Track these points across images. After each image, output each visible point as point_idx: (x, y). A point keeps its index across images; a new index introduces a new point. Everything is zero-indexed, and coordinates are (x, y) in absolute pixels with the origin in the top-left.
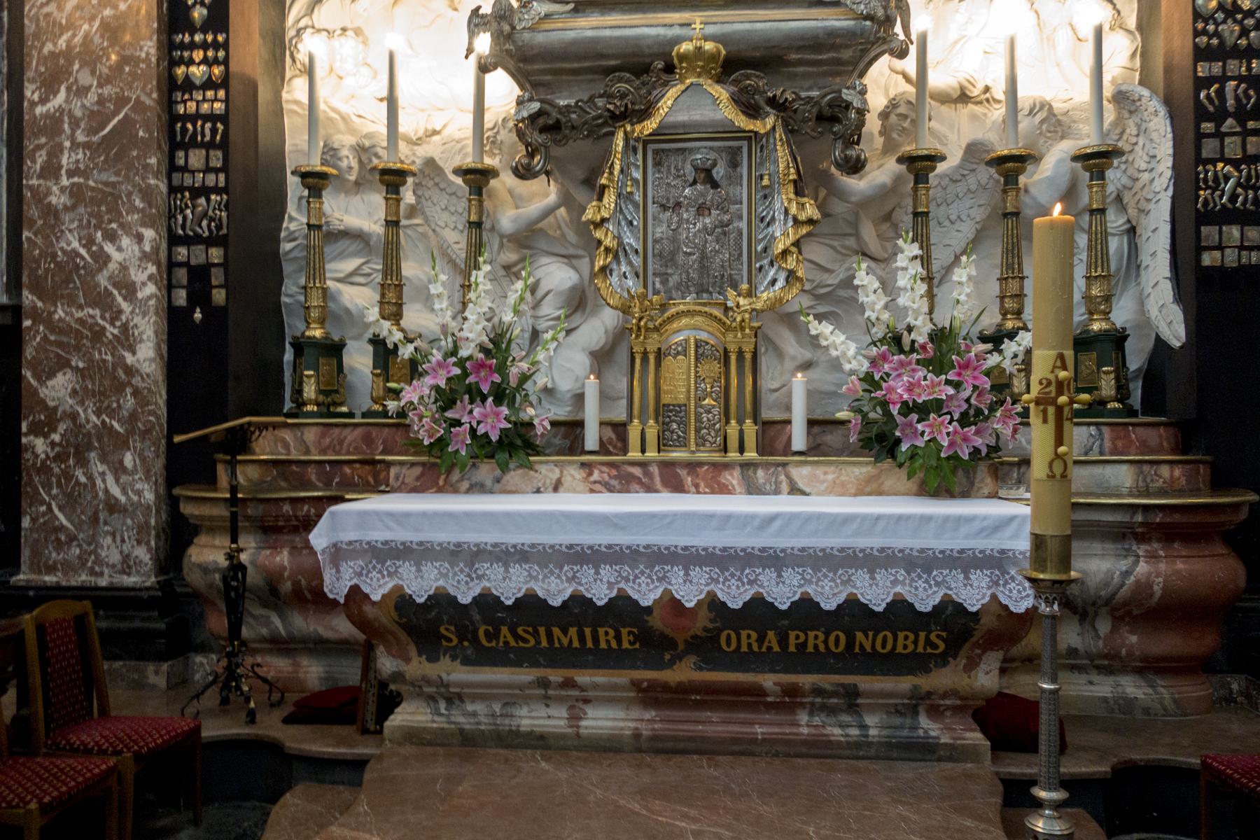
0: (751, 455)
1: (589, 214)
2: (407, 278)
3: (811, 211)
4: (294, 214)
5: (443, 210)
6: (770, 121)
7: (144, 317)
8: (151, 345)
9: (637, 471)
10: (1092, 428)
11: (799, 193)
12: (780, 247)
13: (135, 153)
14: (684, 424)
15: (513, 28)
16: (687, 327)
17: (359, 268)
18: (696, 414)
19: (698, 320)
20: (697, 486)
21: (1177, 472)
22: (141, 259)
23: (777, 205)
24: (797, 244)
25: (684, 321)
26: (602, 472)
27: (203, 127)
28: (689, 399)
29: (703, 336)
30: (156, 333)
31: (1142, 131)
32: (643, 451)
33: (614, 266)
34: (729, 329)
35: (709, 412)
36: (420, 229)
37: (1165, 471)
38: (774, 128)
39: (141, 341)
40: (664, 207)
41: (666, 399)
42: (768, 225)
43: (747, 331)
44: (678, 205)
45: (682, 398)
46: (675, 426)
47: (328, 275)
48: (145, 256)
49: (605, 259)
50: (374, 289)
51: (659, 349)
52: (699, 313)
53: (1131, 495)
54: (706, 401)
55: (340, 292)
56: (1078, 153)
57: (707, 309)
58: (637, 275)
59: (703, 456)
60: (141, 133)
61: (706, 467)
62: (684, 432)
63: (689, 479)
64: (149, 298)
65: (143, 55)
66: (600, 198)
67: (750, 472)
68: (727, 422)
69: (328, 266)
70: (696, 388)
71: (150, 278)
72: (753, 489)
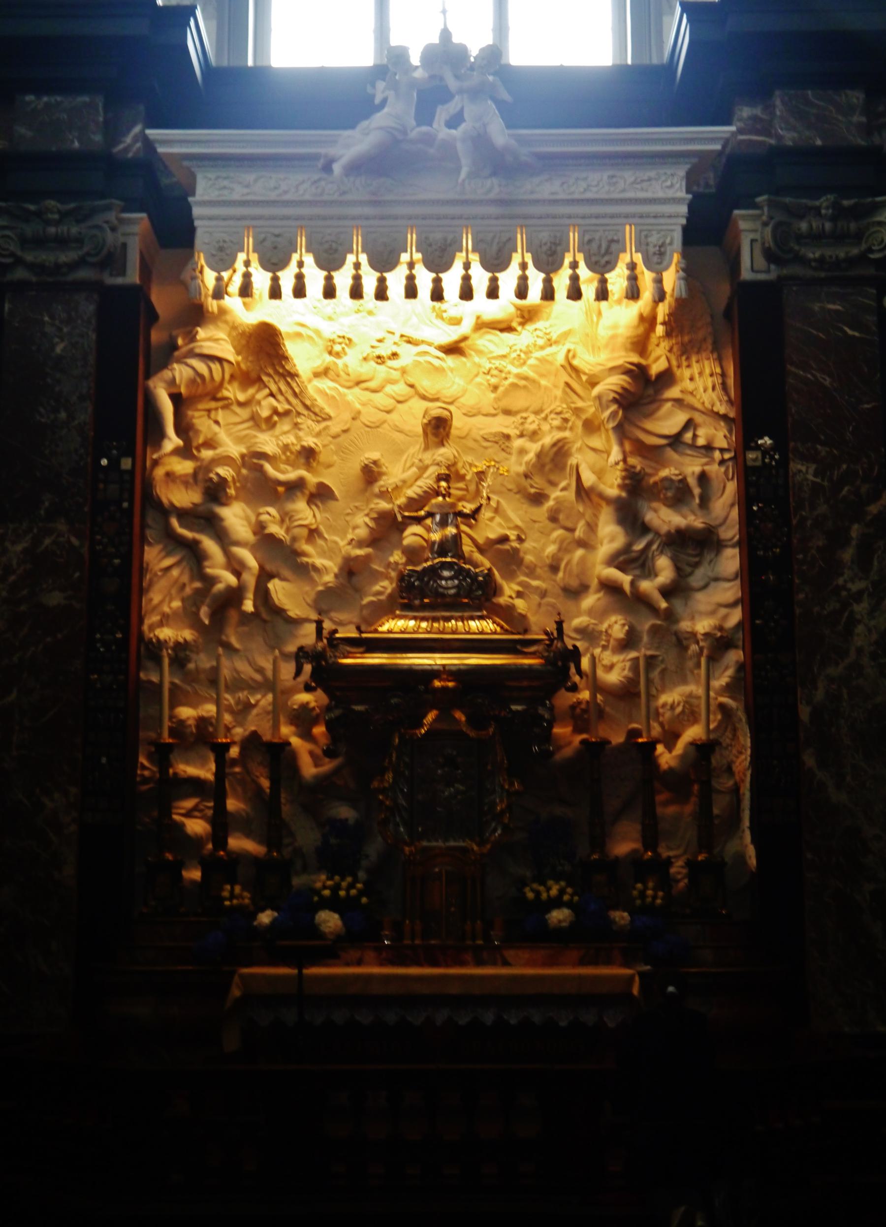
1: (375, 784)
4: (146, 763)
6: (491, 730)
15: (326, 661)
17: (196, 806)
47: (174, 811)
54: (453, 909)
72: (480, 963)
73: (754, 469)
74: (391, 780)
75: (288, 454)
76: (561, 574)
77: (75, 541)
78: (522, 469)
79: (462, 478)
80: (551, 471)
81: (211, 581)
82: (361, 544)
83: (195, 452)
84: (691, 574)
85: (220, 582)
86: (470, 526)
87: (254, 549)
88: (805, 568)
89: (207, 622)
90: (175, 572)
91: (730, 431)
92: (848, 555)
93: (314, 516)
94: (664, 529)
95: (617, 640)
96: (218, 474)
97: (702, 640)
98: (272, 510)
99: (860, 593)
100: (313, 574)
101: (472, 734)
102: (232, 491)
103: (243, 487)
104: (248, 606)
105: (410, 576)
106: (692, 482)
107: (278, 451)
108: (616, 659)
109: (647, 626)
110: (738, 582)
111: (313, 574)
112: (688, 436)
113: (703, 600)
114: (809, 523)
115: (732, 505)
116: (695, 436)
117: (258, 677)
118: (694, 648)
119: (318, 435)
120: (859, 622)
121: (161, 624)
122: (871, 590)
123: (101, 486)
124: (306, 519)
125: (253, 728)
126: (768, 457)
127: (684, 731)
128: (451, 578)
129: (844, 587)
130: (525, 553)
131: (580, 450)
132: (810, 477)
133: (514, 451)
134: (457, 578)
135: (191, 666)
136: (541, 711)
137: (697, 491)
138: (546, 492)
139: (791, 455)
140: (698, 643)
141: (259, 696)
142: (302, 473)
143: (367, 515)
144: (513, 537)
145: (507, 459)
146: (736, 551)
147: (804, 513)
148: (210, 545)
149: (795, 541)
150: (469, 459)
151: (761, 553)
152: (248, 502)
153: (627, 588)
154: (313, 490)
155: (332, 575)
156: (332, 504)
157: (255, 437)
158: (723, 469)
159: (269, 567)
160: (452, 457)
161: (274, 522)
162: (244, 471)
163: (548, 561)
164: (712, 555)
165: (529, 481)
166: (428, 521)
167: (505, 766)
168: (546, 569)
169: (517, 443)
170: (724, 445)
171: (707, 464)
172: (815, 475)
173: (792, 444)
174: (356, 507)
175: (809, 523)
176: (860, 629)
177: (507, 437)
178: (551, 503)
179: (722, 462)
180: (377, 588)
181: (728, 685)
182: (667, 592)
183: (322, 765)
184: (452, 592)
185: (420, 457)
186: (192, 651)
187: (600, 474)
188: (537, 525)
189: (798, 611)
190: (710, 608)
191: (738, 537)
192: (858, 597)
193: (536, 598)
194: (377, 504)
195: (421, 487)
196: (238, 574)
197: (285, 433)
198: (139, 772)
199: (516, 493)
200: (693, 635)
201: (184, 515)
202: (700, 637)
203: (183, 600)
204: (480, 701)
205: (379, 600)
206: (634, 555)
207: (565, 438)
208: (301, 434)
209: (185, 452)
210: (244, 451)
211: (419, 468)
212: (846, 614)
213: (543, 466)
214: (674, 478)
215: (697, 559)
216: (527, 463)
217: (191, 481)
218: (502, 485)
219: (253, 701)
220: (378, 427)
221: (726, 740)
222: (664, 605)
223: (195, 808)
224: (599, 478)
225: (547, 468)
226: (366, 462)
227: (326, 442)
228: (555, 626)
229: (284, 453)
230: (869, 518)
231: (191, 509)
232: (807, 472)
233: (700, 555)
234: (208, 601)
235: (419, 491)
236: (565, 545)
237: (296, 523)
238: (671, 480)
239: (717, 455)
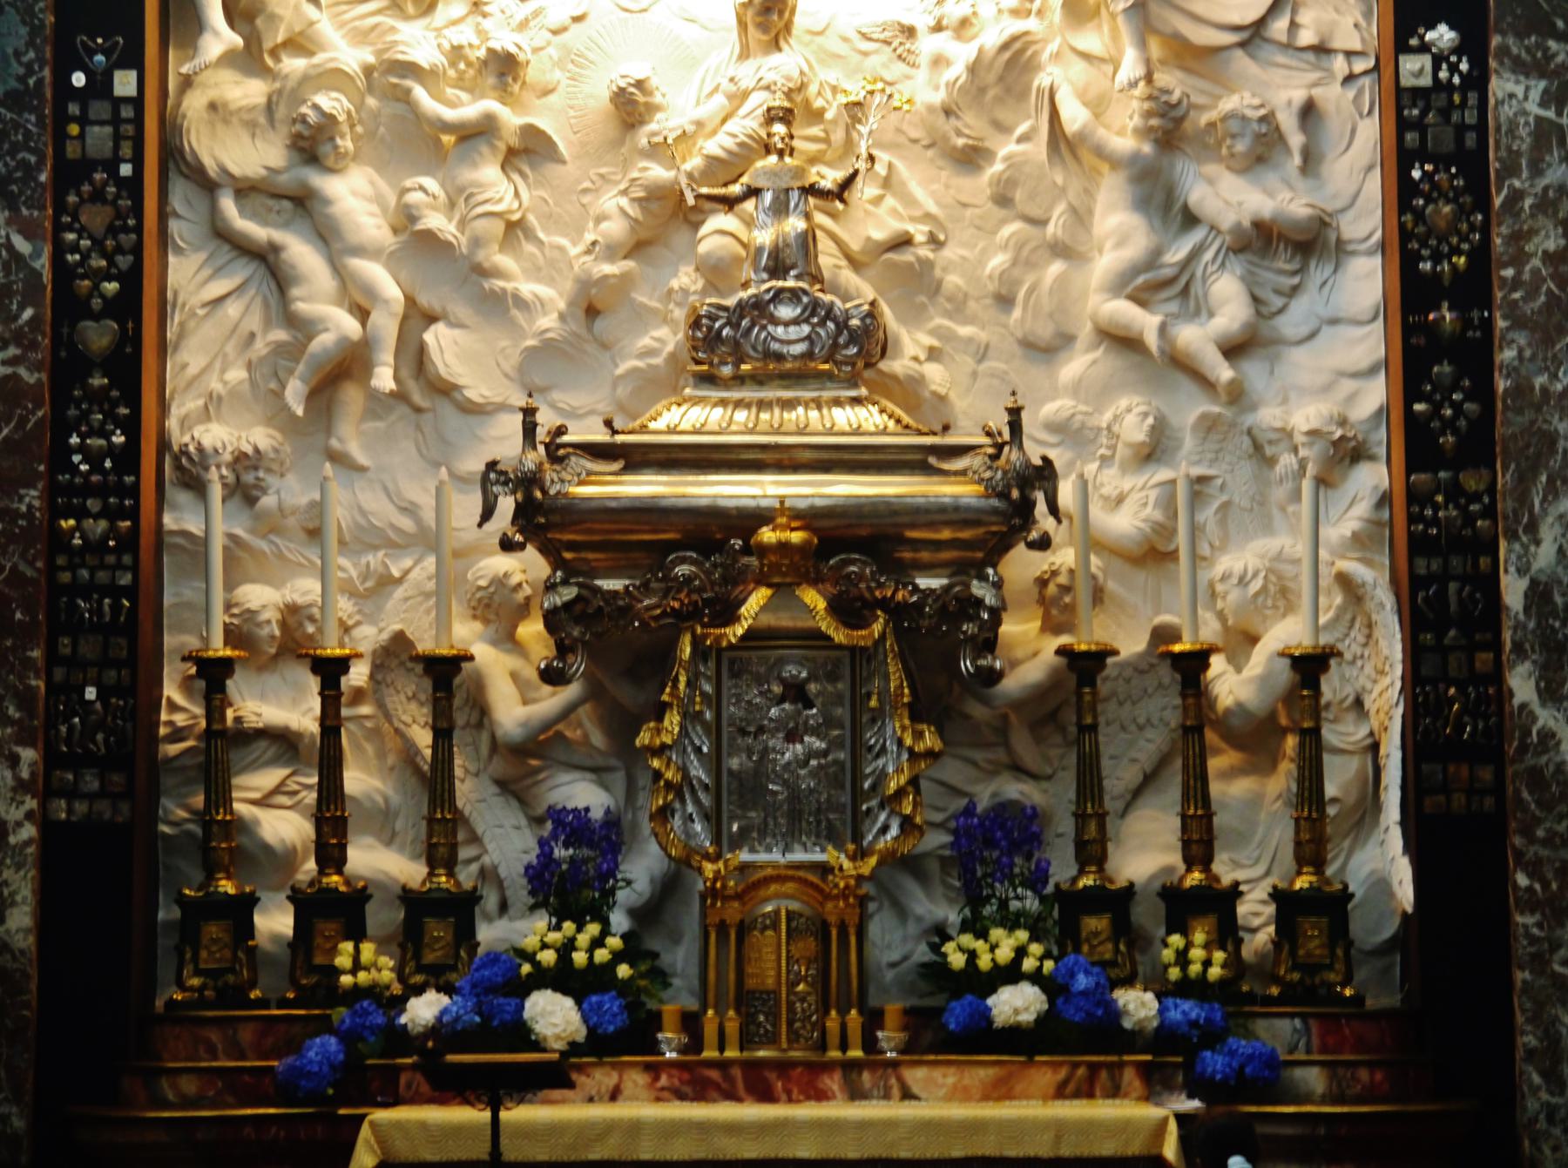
0: (856, 1053)
2: (353, 799)
3: (930, 740)
4: (179, 699)
5: (409, 699)
6: (877, 628)
7: (18, 870)
8: (27, 909)
9: (714, 1074)
11: (915, 717)
12: (893, 786)
13: (9, 643)
14: (774, 1016)
15: (544, 492)
16: (777, 896)
17: (282, 783)
18: (788, 1002)
19: (790, 887)
20: (789, 1093)
22: (14, 790)
23: (889, 732)
24: (914, 782)
25: (773, 888)
26: (670, 1076)
27: (100, 603)
28: (779, 983)
29: (795, 906)
30: (33, 891)
32: (722, 1049)
33: (677, 805)
34: (828, 897)
35: (803, 1000)
36: (369, 724)
37: (1364, 1074)
38: (883, 636)
39: (13, 904)
40: (743, 732)
41: (751, 983)
42: (878, 756)
43: (851, 900)
44: (761, 730)
45: (770, 982)
46: (762, 1018)
47: (234, 795)
48: (21, 787)
49: (665, 798)
50: (302, 814)
51: (742, 921)
52: (792, 879)
53: (1324, 1100)
54: (801, 987)
55: (257, 822)
57: (801, 874)
58: (706, 817)
59: (795, 1054)
60: (18, 616)
61: (799, 1070)
62: (774, 1025)
63: (780, 1084)
64: (27, 843)
65: (24, 508)
66: (660, 719)
67: (854, 1076)
68: (827, 1012)
69: (236, 781)
70: (788, 972)
71: (29, 815)
72: (856, 1094)
73: (1417, 93)
74: (677, 730)
75: (462, 66)
76: (1017, 313)
77: (22, 245)
78: (938, 97)
79: (817, 116)
80: (999, 100)
81: (303, 328)
82: (612, 252)
83: (269, 61)
84: (1281, 311)
85: (326, 330)
86: (833, 215)
87: (392, 261)
88: (1517, 295)
89: (300, 412)
90: (233, 309)
91: (1367, 15)
93: (517, 194)
94: (1227, 220)
95: (1129, 445)
96: (316, 107)
97: (1303, 444)
98: (430, 183)
100: (515, 312)
101: (840, 636)
102: (346, 143)
103: (371, 134)
104: (384, 379)
105: (713, 318)
106: (1288, 122)
107: (440, 60)
108: (1127, 483)
109: (1192, 417)
111: (515, 312)
112: (1279, 27)
113: (1303, 364)
114: (1528, 202)
115: (1370, 168)
116: (1294, 26)
117: (406, 524)
118: (1287, 461)
119: (523, 25)
121: (206, 415)
123: (74, 129)
124: (500, 200)
125: (397, 627)
126: (1444, 66)
128: (796, 322)
130: (945, 270)
131: (1056, 56)
132: (1533, 108)
133: (924, 60)
134: (807, 321)
135: (268, 501)
136: (978, 589)
137: (1296, 140)
138: (987, 144)
139: (1493, 64)
140: (1295, 450)
141: (408, 563)
142: (491, 105)
143: (624, 192)
144: (920, 238)
145: (908, 77)
146: (1377, 261)
147: (1517, 184)
148: (301, 252)
149: (1498, 241)
150: (831, 75)
151: (1426, 266)
152: (380, 168)
153: (1152, 340)
154: (514, 141)
155: (555, 315)
156: (553, 170)
157: (393, 29)
158: (1351, 93)
159: (424, 300)
160: (796, 74)
161: (435, 208)
162: (371, 102)
163: (992, 287)
164: (1329, 269)
165: (953, 121)
166: (749, 205)
167: (906, 700)
168: (988, 301)
169: (928, 44)
170: (1357, 46)
171: (1315, 85)
172: (1543, 104)
173: (1496, 40)
174: (602, 176)
175: (1528, 202)
177: (910, 32)
178: (998, 167)
179: (1350, 78)
180: (646, 341)
181: (1356, 536)
182: (1233, 350)
183: (535, 701)
184: (798, 349)
185: (730, 74)
186: (269, 470)
187: (1097, 105)
188: (969, 212)
189: (1501, 384)
193: (968, 362)
194: (645, 169)
195: (735, 136)
196: (363, 314)
197: (455, 23)
198: (164, 717)
199: (928, 147)
200: (1287, 434)
201: (246, 190)
202: (1299, 439)
203: (249, 366)
204: (853, 568)
205: (650, 366)
206: (1167, 272)
207: (1026, 33)
208: (487, 24)
209: (250, 59)
210: (371, 59)
211: (730, 97)
213: (982, 90)
214: (1250, 113)
215: (1296, 280)
216: (950, 86)
217: (262, 120)
218: (899, 131)
219: (396, 573)
220: (645, 10)
221: (1350, 648)
222: (1224, 372)
223: (277, 790)
224: (1097, 116)
225: (991, 93)
226: (623, 84)
227: (538, 43)
228: (1006, 418)
229: (453, 64)
231: (263, 179)
232: (1526, 98)
233: (1302, 270)
234: (301, 368)
235: (730, 143)
236: (1025, 253)
237: (480, 210)
238: (1244, 118)
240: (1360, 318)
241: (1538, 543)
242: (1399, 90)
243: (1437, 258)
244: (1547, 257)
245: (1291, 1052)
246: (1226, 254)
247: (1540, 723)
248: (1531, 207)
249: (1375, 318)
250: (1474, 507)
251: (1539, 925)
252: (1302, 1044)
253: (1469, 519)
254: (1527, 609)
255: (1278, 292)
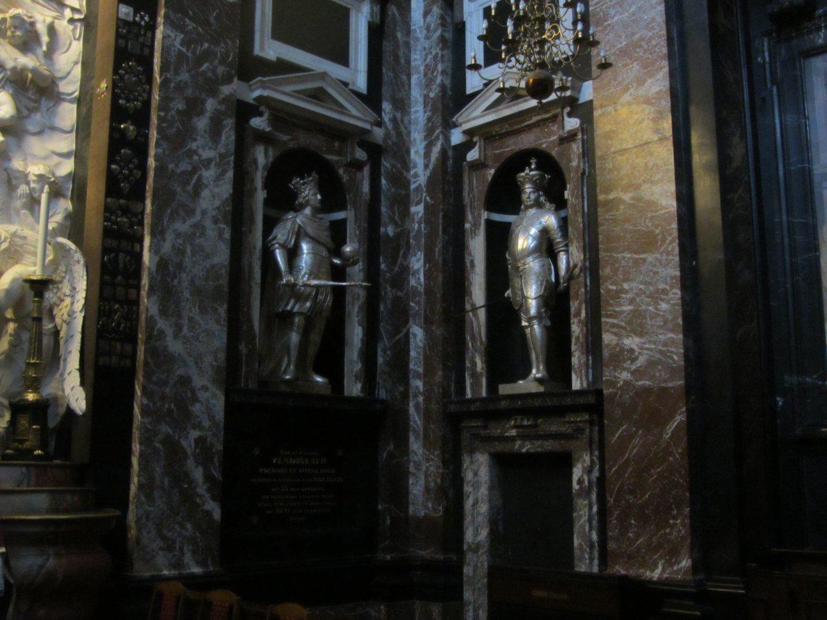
10: (24, 468)
21: (76, 498)
31: (69, 271)
37: (69, 497)
53: (47, 512)
56: (28, 278)
73: (126, 23)
88: (164, 125)
92: (202, 123)
97: (34, 181)
99: (209, 161)
106: (41, 28)
110: (73, 135)
113: (35, 145)
118: (23, 189)
120: (206, 186)
122: (218, 160)
126: (138, 15)
127: (7, 269)
129: (196, 152)
137: (45, 39)
146: (75, 106)
147: (168, 75)
158: (71, 27)
172: (182, 44)
175: (172, 85)
176: (205, 193)
179: (71, 21)
190: (42, 153)
191: (77, 94)
192: (207, 163)
200: (25, 176)
202: (32, 178)
212: (195, 177)
214: (26, 18)
230: (222, 96)
232: (175, 40)
238: (23, 20)
239: (68, 13)
240: (65, 129)
241: (164, 240)
242: (118, 19)
243: (128, 100)
244: (178, 112)
245: (19, 486)
246: (6, 81)
247: (159, 325)
248: (173, 87)
249: (70, 132)
250: (134, 219)
251: (150, 423)
252: (25, 482)
253: (131, 226)
254: (157, 270)
255: (28, 109)
